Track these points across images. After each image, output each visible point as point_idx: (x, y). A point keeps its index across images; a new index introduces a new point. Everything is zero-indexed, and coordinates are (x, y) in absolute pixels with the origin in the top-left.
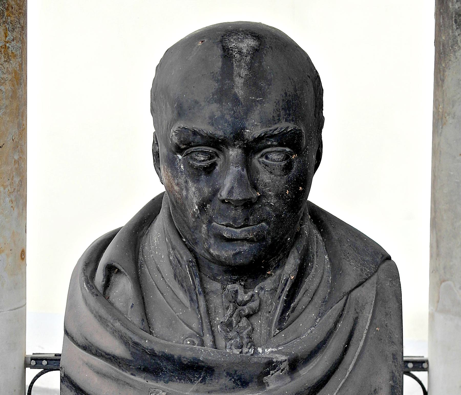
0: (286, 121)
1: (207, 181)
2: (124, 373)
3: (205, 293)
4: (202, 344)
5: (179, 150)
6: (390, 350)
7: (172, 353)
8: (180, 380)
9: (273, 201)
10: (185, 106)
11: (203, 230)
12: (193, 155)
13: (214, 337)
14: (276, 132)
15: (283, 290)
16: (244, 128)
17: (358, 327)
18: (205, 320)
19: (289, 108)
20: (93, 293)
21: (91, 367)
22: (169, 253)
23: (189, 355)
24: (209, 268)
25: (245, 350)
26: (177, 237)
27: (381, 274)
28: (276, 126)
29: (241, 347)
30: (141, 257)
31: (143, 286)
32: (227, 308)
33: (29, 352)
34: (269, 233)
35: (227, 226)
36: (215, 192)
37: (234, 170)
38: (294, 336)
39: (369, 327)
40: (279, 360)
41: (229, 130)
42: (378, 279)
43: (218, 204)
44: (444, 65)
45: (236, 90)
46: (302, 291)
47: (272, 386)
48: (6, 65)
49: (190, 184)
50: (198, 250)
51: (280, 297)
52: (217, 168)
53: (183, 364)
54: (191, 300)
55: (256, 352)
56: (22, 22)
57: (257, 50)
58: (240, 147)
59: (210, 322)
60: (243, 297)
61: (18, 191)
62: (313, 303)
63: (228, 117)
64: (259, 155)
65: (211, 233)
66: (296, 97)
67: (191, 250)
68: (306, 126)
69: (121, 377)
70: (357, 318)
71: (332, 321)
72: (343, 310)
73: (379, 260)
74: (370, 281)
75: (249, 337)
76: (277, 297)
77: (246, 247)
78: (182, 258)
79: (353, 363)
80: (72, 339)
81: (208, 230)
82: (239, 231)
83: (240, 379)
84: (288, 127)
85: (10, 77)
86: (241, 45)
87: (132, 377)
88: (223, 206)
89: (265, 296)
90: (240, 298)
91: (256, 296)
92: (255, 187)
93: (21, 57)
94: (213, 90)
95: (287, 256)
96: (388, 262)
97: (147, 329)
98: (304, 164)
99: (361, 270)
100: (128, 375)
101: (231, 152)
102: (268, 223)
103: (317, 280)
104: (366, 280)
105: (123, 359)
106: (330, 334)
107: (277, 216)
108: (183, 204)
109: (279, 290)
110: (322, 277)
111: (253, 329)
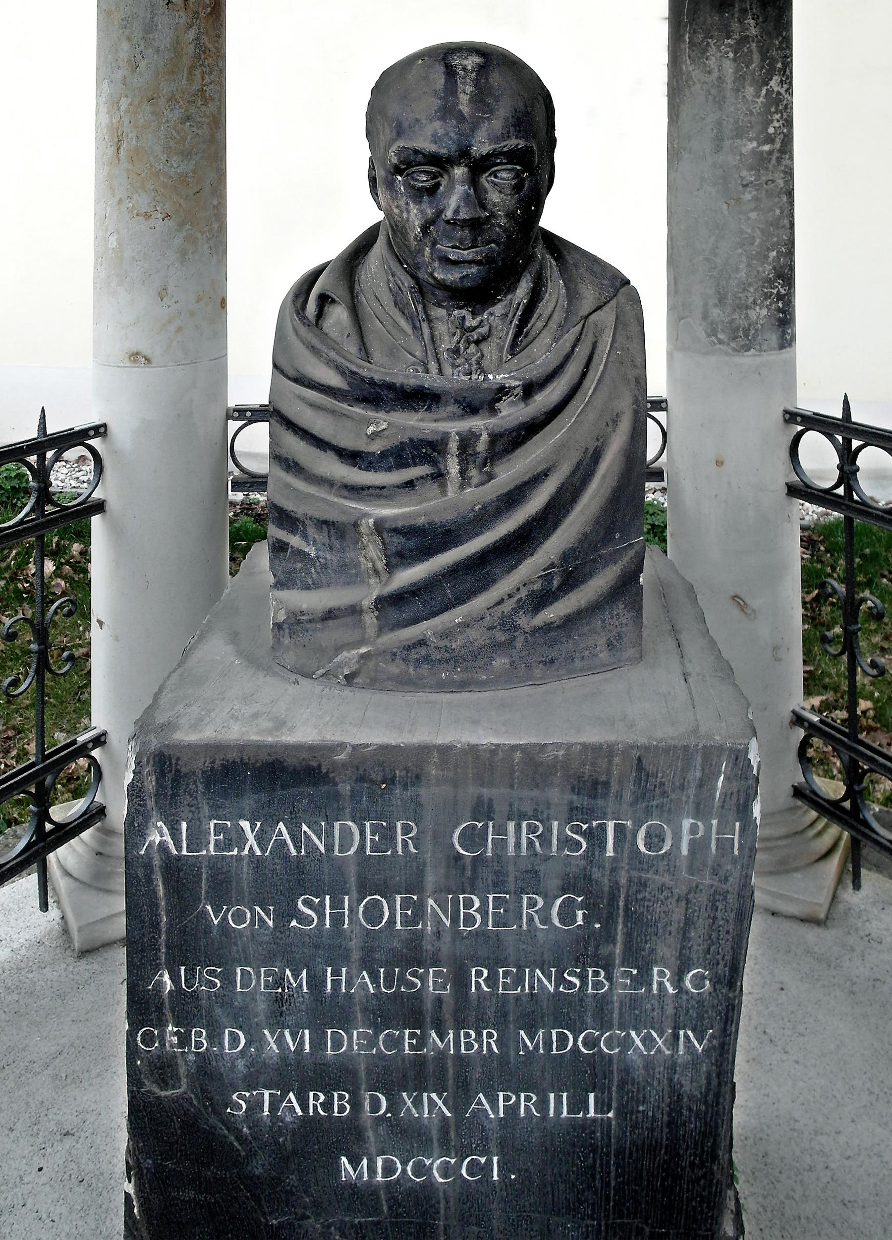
0: (516, 138)
1: (431, 203)
2: (340, 404)
3: (429, 320)
4: (427, 371)
5: (398, 170)
6: (632, 374)
7: (394, 381)
8: (403, 409)
9: (503, 222)
10: (405, 125)
11: (426, 253)
12: (415, 175)
13: (440, 365)
14: (505, 149)
15: (515, 314)
16: (471, 146)
17: (598, 352)
18: (430, 348)
19: (519, 125)
20: (304, 324)
21: (302, 399)
22: (389, 280)
23: (413, 382)
24: (433, 294)
25: (474, 377)
26: (398, 264)
27: (621, 298)
28: (505, 143)
29: (470, 374)
30: (357, 287)
31: (360, 316)
32: (454, 335)
33: (231, 404)
34: (499, 255)
35: (453, 247)
36: (440, 213)
37: (460, 189)
38: (528, 362)
39: (609, 351)
40: (513, 385)
41: (454, 147)
42: (618, 303)
43: (442, 225)
44: (678, 100)
45: (461, 107)
46: (535, 316)
47: (504, 413)
48: (203, 108)
49: (412, 205)
50: (420, 275)
51: (511, 322)
52: (441, 188)
53: (406, 391)
54: (414, 327)
55: (486, 379)
56: (220, 65)
57: (482, 67)
58: (466, 166)
59: (435, 349)
60: (470, 322)
61: (217, 237)
62: (547, 328)
63: (452, 135)
64: (487, 174)
65: (435, 256)
66: (527, 114)
67: (414, 277)
68: (539, 144)
69: (337, 409)
70: (596, 342)
71: (568, 346)
72: (581, 334)
73: (618, 284)
74: (609, 305)
75: (478, 363)
76: (508, 320)
77: (474, 269)
78: (403, 284)
79: (593, 387)
80: (282, 372)
81: (431, 253)
82: (466, 252)
83: (469, 405)
84: (518, 145)
85: (207, 120)
86: (465, 62)
87: (350, 408)
88: (448, 227)
89: (496, 321)
90: (467, 324)
91: (485, 322)
92: (483, 207)
93: (220, 100)
94: (436, 108)
95: (519, 281)
96: (627, 286)
97: (366, 358)
98: (537, 183)
99: (600, 294)
100: (345, 406)
101: (456, 171)
102: (498, 244)
103: (551, 306)
104: (605, 304)
105: (339, 390)
106: (567, 358)
107: (507, 237)
108: (403, 227)
109: (510, 316)
110: (557, 302)
111: (483, 355)
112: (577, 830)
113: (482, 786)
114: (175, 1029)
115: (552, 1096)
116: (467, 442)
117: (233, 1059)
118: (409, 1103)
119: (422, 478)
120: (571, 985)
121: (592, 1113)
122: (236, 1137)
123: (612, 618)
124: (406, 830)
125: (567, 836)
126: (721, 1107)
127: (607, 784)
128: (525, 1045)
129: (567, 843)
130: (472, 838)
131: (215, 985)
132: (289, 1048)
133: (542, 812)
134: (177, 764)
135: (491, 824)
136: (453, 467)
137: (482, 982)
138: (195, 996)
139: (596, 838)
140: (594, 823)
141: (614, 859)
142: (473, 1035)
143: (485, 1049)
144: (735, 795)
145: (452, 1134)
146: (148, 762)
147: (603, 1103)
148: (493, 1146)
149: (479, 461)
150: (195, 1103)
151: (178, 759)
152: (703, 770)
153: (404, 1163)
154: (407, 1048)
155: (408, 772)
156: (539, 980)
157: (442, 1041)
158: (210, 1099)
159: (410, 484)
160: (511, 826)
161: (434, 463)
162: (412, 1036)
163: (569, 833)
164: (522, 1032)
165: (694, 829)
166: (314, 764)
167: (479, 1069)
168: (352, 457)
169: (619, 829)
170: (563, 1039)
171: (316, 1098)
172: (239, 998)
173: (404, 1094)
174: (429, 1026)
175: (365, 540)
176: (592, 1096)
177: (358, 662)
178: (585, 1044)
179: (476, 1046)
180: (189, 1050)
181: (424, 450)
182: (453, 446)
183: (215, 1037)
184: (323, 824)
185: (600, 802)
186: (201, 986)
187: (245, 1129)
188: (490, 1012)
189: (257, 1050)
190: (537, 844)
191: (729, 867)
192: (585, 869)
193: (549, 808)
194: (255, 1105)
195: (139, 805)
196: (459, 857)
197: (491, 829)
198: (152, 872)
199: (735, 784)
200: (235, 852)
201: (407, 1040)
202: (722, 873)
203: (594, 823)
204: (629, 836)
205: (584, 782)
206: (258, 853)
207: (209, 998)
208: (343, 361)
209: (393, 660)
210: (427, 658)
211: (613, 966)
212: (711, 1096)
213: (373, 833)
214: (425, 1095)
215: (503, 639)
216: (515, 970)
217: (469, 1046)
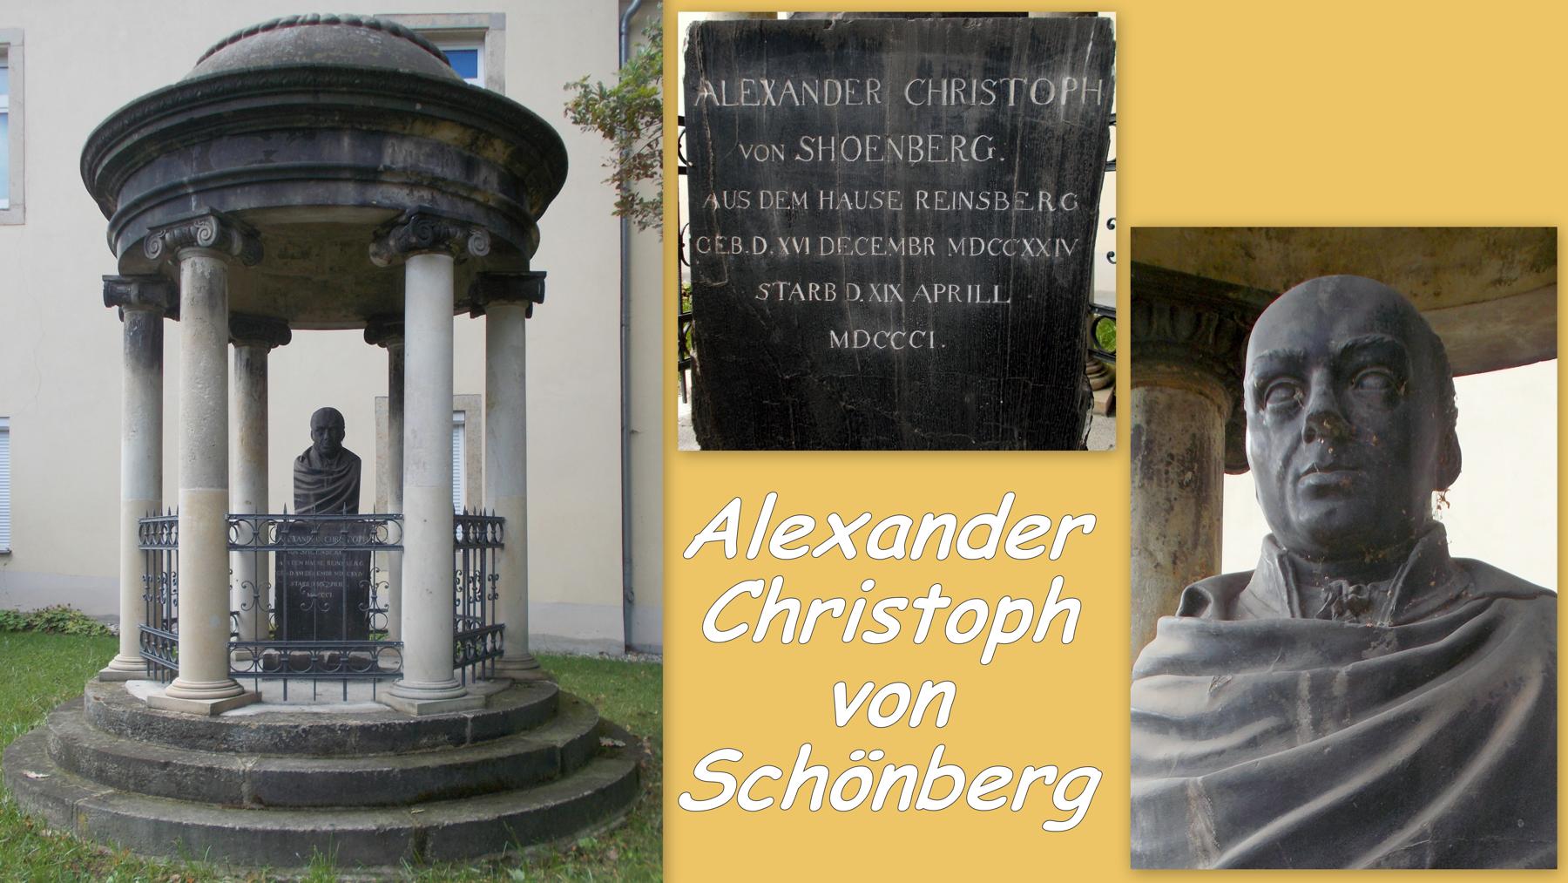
112: (989, 86)
115: (970, 287)
120: (984, 204)
121: (996, 301)
124: (873, 86)
127: (1010, 49)
130: (919, 92)
131: (746, 204)
132: (795, 251)
135: (930, 81)
138: (734, 212)
139: (1002, 91)
140: (1001, 81)
142: (918, 241)
145: (903, 315)
148: (930, 323)
150: (734, 291)
151: (718, 32)
153: (872, 336)
155: (874, 40)
156: (962, 200)
157: (897, 245)
160: (945, 83)
162: (877, 242)
163: (984, 88)
164: (950, 240)
165: (1070, 85)
167: (921, 266)
170: (977, 245)
171: (814, 288)
174: (887, 235)
176: (996, 287)
178: (992, 248)
179: (920, 250)
185: (1005, 64)
187: (767, 310)
192: (994, 115)
194: (774, 292)
197: (930, 85)
198: (702, 120)
199: (1100, 48)
204: (1025, 91)
206: (774, 104)
207: (742, 213)
211: (1012, 189)
212: (1075, 288)
213: (850, 89)
214: (886, 286)
216: (946, 193)
217: (915, 250)
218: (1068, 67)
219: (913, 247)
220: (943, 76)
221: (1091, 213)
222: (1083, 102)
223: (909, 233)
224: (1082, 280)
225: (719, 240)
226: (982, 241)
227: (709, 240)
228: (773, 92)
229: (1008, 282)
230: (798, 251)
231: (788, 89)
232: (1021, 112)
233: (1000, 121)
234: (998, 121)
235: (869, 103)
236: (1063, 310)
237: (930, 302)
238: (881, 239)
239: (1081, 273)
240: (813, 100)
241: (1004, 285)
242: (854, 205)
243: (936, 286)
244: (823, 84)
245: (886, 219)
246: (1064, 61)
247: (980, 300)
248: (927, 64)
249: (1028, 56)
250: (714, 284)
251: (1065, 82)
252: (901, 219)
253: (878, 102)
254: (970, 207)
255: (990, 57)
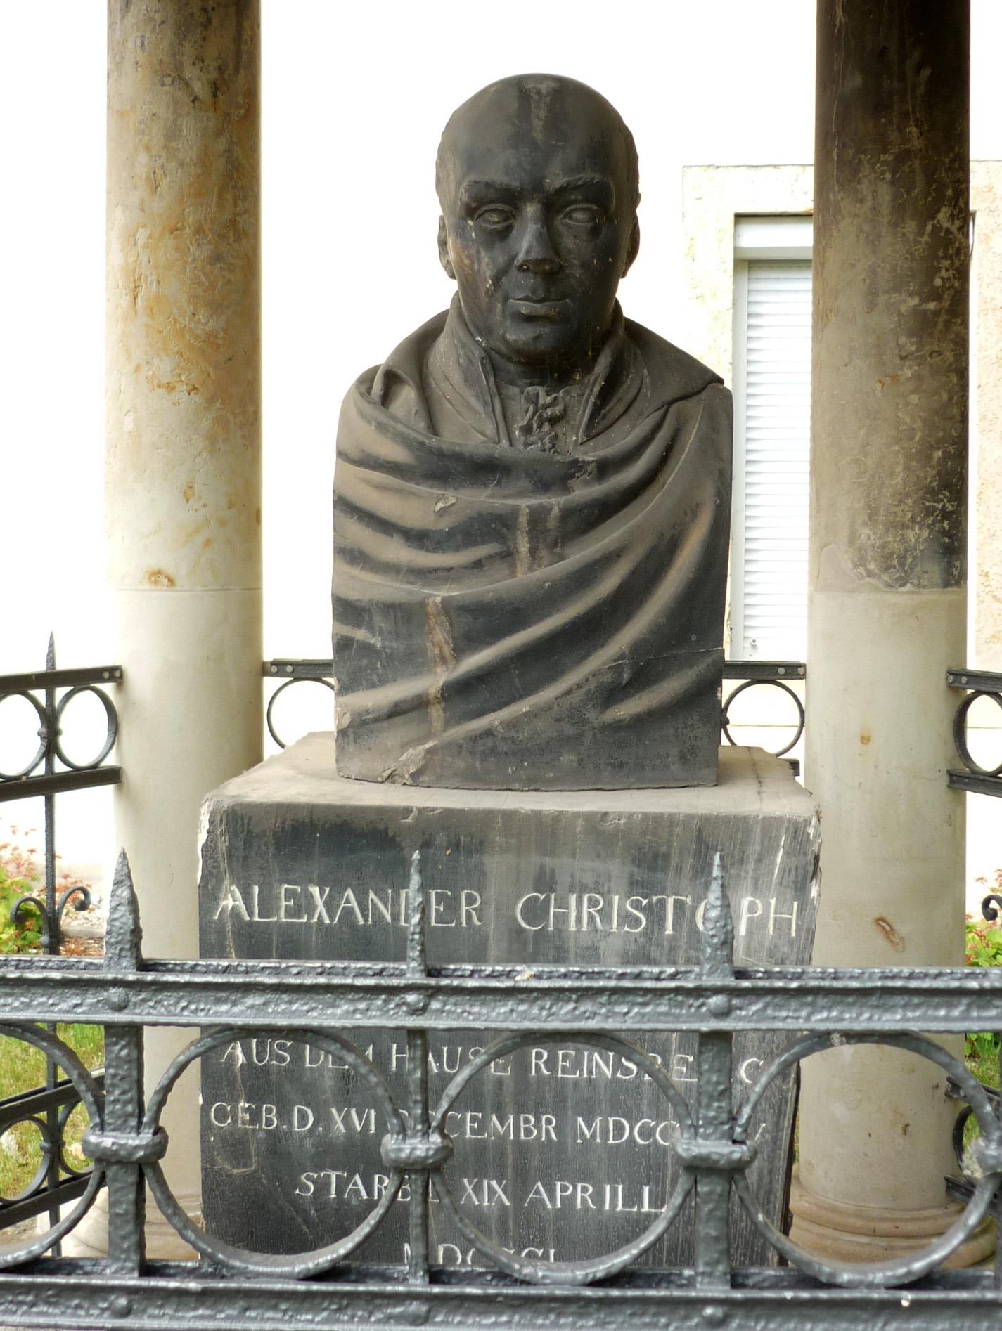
9: (578, 273)
12: (486, 215)
36: (514, 258)
43: (514, 271)
112: (637, 905)
113: (545, 855)
114: (247, 1105)
115: (608, 1188)
116: (537, 518)
117: (303, 1137)
118: (470, 1189)
119: (491, 556)
120: (627, 1071)
121: (646, 1208)
122: (304, 1220)
123: (685, 728)
124: (470, 900)
125: (627, 912)
126: (772, 1205)
127: (667, 857)
128: (582, 1133)
129: (627, 918)
130: (535, 911)
131: (284, 1060)
132: (355, 1128)
133: (603, 886)
134: (249, 824)
135: (553, 896)
136: (523, 546)
137: (542, 1066)
138: (266, 1070)
139: (655, 913)
140: (655, 899)
141: (673, 938)
142: (533, 1120)
143: (544, 1136)
144: (793, 871)
145: (511, 1223)
146: (221, 821)
147: (657, 1196)
148: (550, 1238)
149: (549, 539)
150: (264, 1181)
151: (250, 819)
152: (762, 843)
153: (464, 1253)
154: (468, 1132)
155: (472, 839)
156: (597, 1065)
157: (502, 1125)
158: (279, 1179)
159: (478, 564)
160: (573, 899)
161: (501, 538)
162: (473, 1119)
163: (629, 908)
164: (580, 1120)
165: (752, 908)
166: (382, 827)
167: (537, 1156)
168: (418, 538)
169: (679, 905)
170: (619, 1128)
171: (381, 1181)
172: (308, 1073)
173: (465, 1181)
174: (489, 1110)
175: (432, 621)
176: (646, 1190)
177: (424, 758)
178: (641, 1134)
179: (535, 1132)
180: (260, 1126)
181: (493, 526)
182: (523, 520)
183: (284, 1115)
184: (390, 891)
185: (659, 876)
186: (271, 1060)
187: (313, 1212)
188: (549, 1097)
189: (325, 1129)
190: (598, 919)
191: (786, 949)
192: (644, 947)
193: (610, 881)
194: (322, 1186)
195: (213, 867)
196: (521, 931)
197: (553, 902)
198: (225, 938)
199: (793, 859)
200: (305, 920)
201: (469, 1124)
202: (779, 956)
203: (655, 899)
204: (688, 913)
205: (644, 853)
206: (327, 921)
207: (279, 1073)
208: (410, 432)
209: (459, 753)
210: (493, 751)
211: (669, 1052)
212: (762, 1194)
213: (438, 903)
214: (485, 1182)
215: (571, 732)
216: (574, 1053)
217: (528, 1132)
218: (748, 884)
219: (526, 1129)
220: (571, 891)
221: (784, 1087)
222: (771, 932)
223: (520, 1108)
224: (771, 1182)
225: (242, 1108)
226: (625, 1122)
227: (229, 1108)
228: (327, 904)
229: (664, 1183)
230: (359, 1129)
231: (348, 901)
232: (683, 943)
233: (652, 954)
234: (649, 954)
235: (464, 924)
236: (743, 1224)
237: (550, 1207)
238: (480, 1115)
239: (770, 1172)
240: (384, 917)
241: (657, 1187)
242: (441, 1066)
243: (559, 1184)
244: (399, 895)
245: (489, 1087)
246: (743, 874)
247: (623, 1206)
248: (548, 871)
249: (693, 867)
250: (235, 1171)
251: (745, 903)
252: (509, 1087)
253: (477, 923)
254: (609, 1074)
255: (639, 866)
